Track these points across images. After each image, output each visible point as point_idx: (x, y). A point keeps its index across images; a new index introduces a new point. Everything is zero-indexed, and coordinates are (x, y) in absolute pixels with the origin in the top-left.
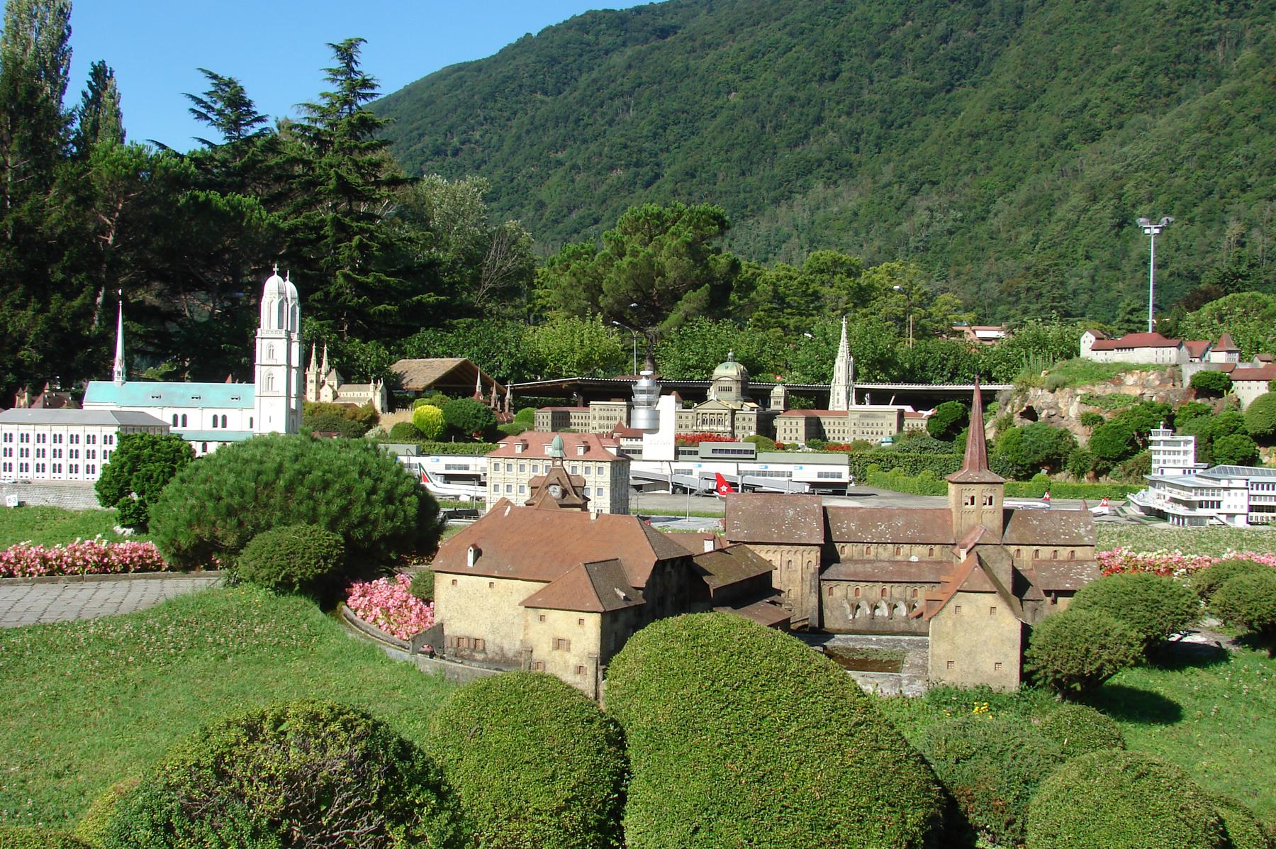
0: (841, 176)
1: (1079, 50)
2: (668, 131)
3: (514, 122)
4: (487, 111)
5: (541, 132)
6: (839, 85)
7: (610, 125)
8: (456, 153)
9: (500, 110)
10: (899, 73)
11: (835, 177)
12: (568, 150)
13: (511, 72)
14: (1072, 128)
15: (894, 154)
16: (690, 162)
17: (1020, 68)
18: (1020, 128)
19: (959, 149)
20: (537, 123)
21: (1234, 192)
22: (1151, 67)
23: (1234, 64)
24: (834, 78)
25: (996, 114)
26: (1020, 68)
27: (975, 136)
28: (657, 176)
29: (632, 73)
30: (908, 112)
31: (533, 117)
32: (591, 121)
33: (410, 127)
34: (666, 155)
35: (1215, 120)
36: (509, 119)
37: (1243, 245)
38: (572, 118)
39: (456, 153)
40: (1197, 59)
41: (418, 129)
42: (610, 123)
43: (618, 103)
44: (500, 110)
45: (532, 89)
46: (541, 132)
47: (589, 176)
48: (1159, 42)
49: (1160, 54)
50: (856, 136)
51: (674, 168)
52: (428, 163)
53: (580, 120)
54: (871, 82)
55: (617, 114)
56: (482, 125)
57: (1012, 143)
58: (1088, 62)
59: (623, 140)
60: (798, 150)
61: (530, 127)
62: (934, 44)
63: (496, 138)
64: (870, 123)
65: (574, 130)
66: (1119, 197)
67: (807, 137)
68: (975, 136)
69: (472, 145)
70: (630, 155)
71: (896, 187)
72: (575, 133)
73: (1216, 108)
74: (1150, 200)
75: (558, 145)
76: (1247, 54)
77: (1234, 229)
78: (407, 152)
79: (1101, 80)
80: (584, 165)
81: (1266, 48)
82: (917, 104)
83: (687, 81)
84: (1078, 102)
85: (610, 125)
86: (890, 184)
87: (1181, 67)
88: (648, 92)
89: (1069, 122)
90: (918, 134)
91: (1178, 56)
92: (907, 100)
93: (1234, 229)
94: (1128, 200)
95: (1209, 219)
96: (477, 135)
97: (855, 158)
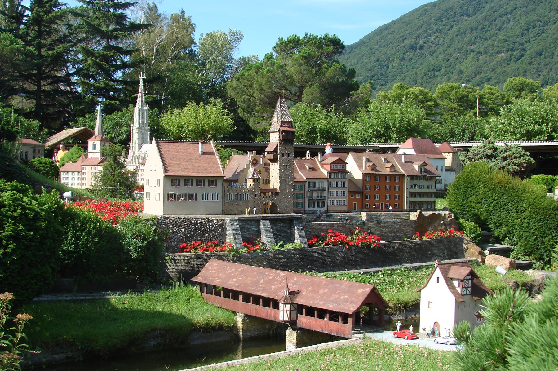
2: (530, 31)
3: (451, 31)
4: (437, 26)
5: (463, 35)
7: (499, 30)
8: (421, 48)
9: (445, 25)
12: (477, 44)
13: (451, 6)
16: (540, 47)
20: (461, 31)
28: (523, 55)
31: (460, 28)
32: (489, 29)
33: (399, 36)
34: (528, 44)
36: (449, 30)
38: (480, 27)
39: (421, 48)
41: (403, 37)
42: (500, 29)
43: (504, 18)
44: (445, 25)
45: (461, 14)
46: (463, 35)
47: (486, 57)
51: (531, 50)
52: (407, 53)
53: (483, 28)
55: (503, 24)
56: (435, 33)
59: (505, 37)
61: (457, 33)
63: (442, 40)
65: (480, 34)
69: (430, 44)
70: (508, 45)
72: (481, 35)
75: (472, 42)
78: (397, 48)
80: (484, 51)
83: (541, 5)
85: (499, 30)
88: (519, 12)
96: (432, 39)
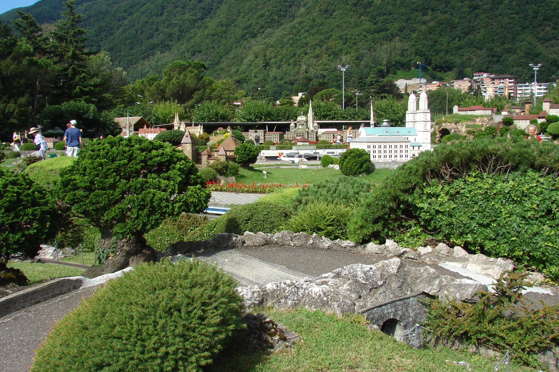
0: (166, 50)
1: (247, 6)
6: (164, 17)
10: (184, 13)
11: (164, 50)
14: (247, 33)
15: (184, 42)
17: (227, 12)
18: (229, 32)
19: (208, 40)
21: (302, 55)
22: (272, 13)
23: (298, 13)
24: (161, 15)
25: (220, 28)
26: (227, 12)
27: (214, 35)
29: (87, 12)
30: (188, 27)
35: (294, 31)
37: (307, 73)
40: (286, 11)
48: (274, 5)
49: (274, 8)
50: (170, 35)
54: (175, 16)
57: (226, 38)
58: (251, 11)
60: (150, 40)
62: (196, 3)
64: (175, 30)
66: (265, 56)
67: (153, 36)
68: (214, 35)
71: (186, 54)
73: (294, 27)
74: (275, 57)
76: (302, 10)
77: (304, 67)
79: (255, 17)
81: (309, 8)
82: (191, 24)
84: (249, 23)
86: (184, 52)
87: (282, 13)
89: (246, 31)
90: (192, 35)
91: (280, 10)
92: (187, 23)
93: (304, 67)
94: (268, 57)
95: (295, 64)
97: (170, 43)
